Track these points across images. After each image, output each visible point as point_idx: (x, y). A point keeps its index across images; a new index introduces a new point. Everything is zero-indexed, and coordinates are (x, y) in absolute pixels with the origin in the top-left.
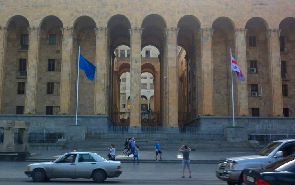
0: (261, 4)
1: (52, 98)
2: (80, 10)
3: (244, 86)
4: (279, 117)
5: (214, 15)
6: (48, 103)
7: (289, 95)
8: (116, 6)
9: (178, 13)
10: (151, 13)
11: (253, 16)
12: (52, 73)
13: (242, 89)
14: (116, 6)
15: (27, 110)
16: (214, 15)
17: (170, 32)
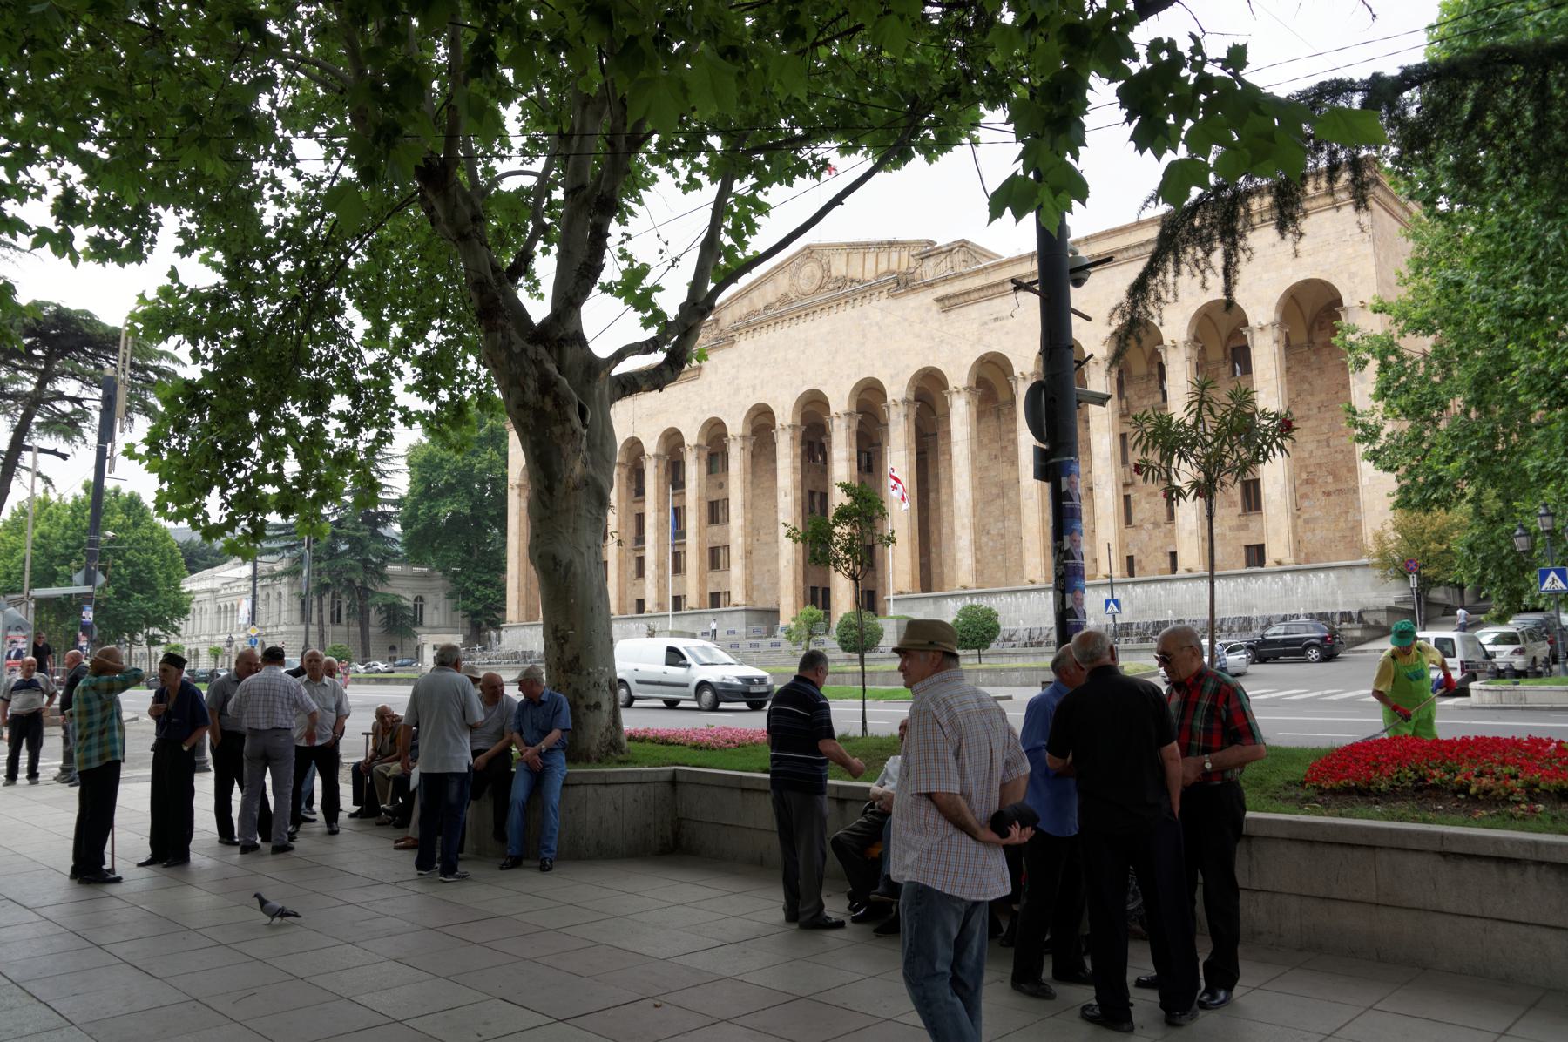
0: (996, 319)
1: (717, 576)
2: (705, 407)
3: (966, 521)
4: (1036, 586)
5: (908, 366)
6: (712, 589)
7: (1134, 521)
8: (754, 388)
9: (849, 377)
10: (805, 389)
11: (983, 351)
12: (715, 528)
13: (963, 526)
14: (754, 388)
15: (648, 606)
16: (908, 366)
17: (836, 422)
